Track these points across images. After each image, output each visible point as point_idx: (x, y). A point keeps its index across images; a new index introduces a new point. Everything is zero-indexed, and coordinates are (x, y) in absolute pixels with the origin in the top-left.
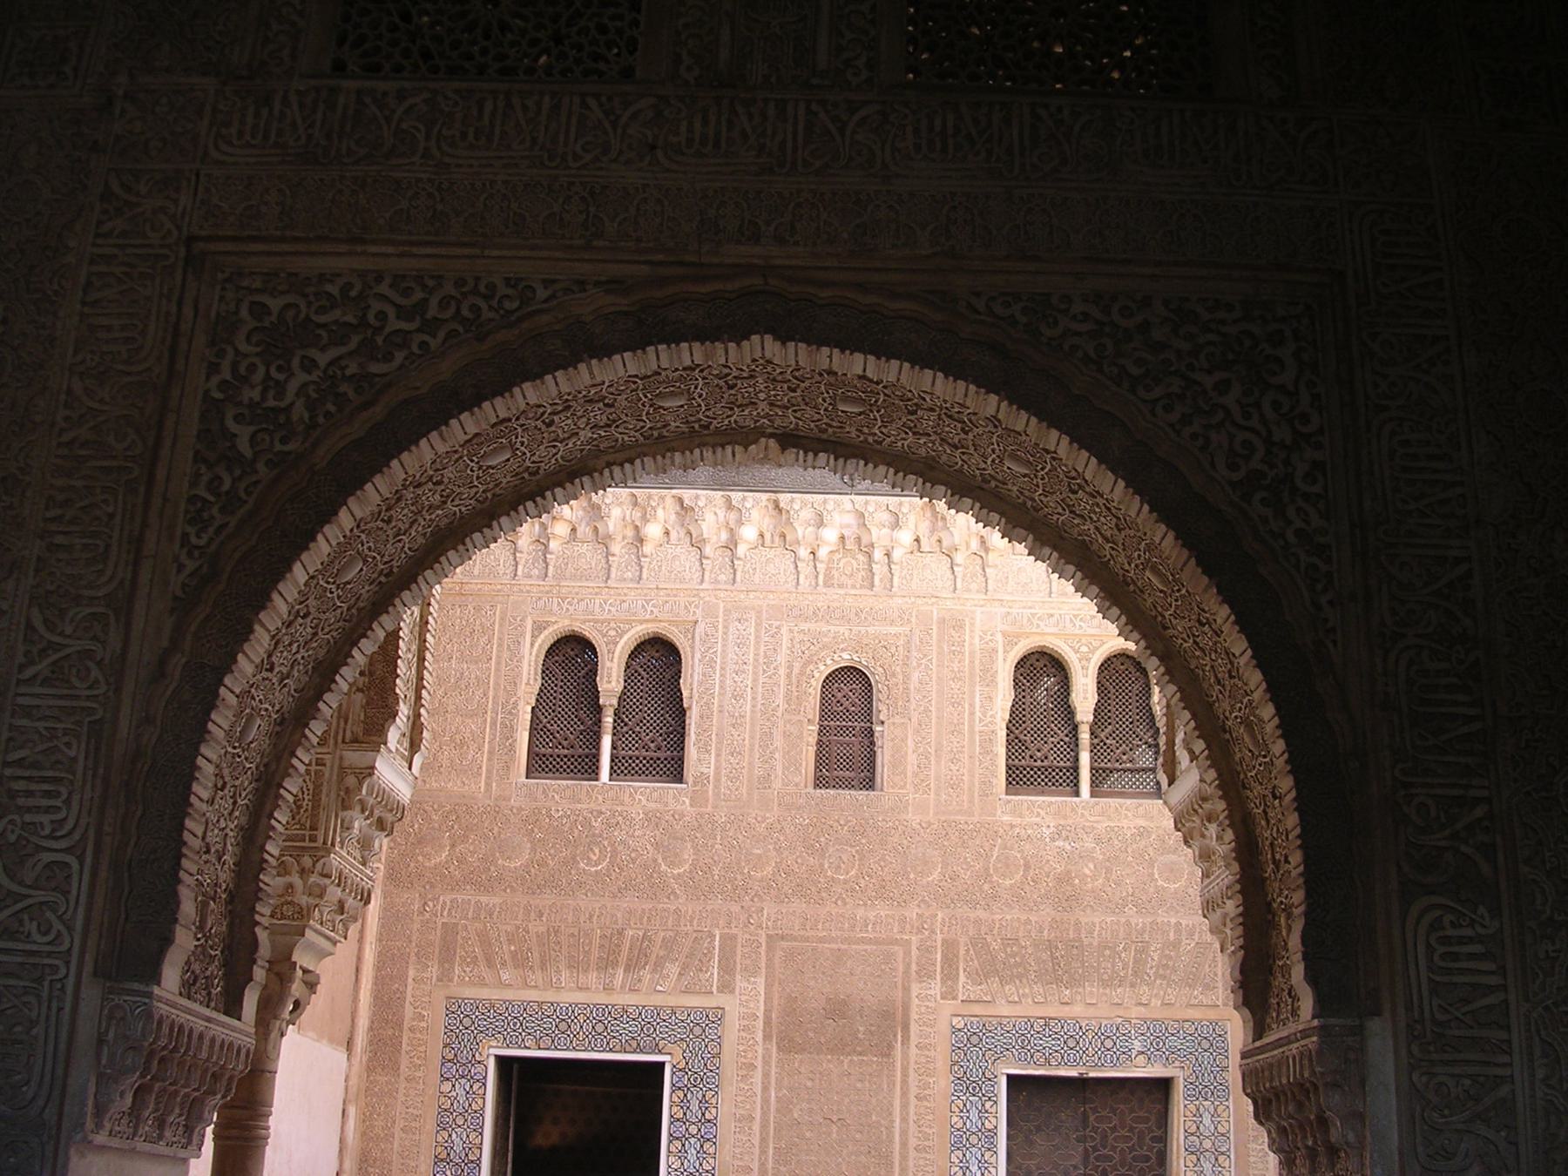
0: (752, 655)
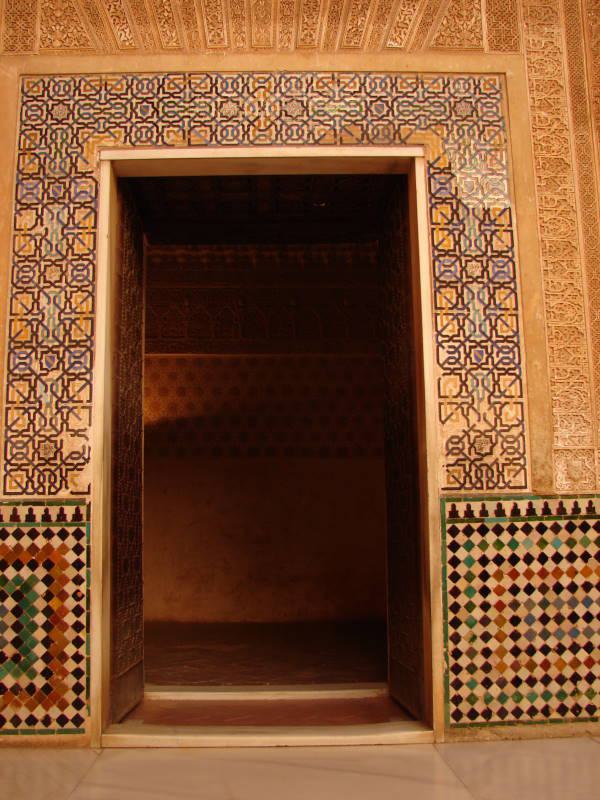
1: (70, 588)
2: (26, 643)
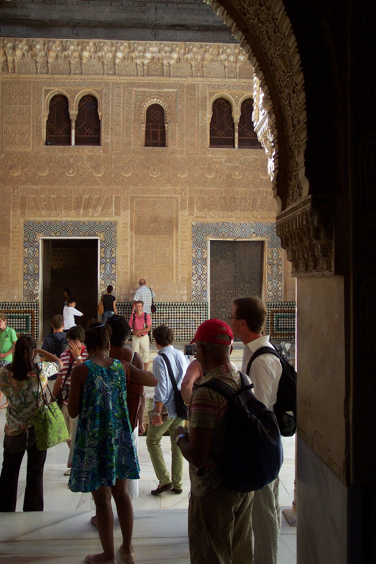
0: (122, 100)
1: (35, 317)
2: (28, 326)
